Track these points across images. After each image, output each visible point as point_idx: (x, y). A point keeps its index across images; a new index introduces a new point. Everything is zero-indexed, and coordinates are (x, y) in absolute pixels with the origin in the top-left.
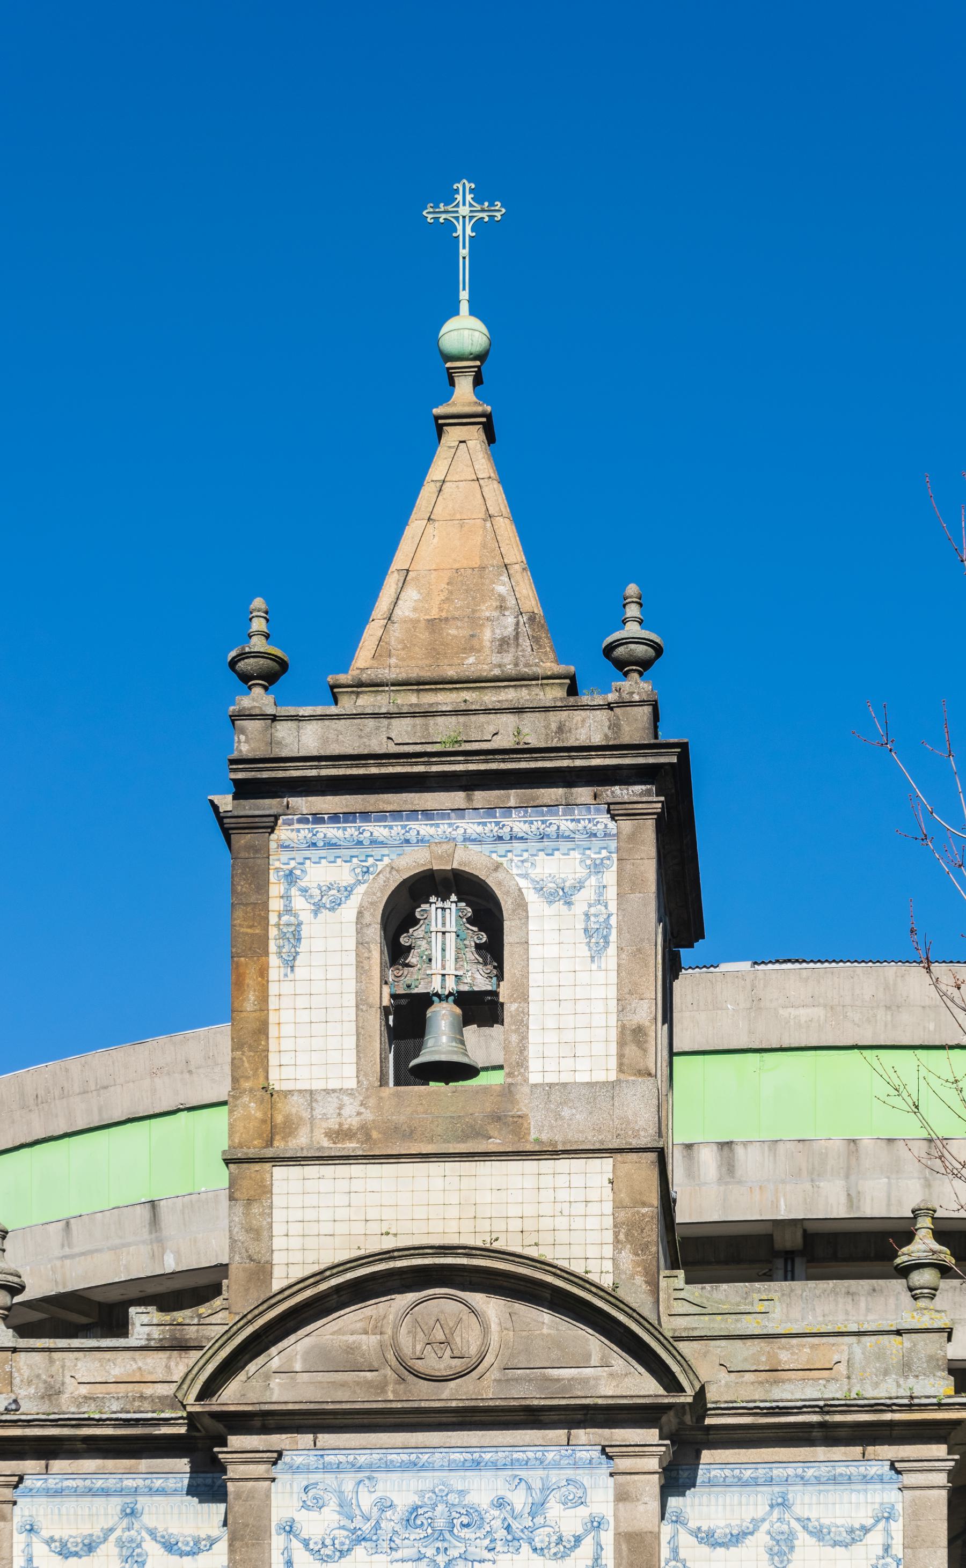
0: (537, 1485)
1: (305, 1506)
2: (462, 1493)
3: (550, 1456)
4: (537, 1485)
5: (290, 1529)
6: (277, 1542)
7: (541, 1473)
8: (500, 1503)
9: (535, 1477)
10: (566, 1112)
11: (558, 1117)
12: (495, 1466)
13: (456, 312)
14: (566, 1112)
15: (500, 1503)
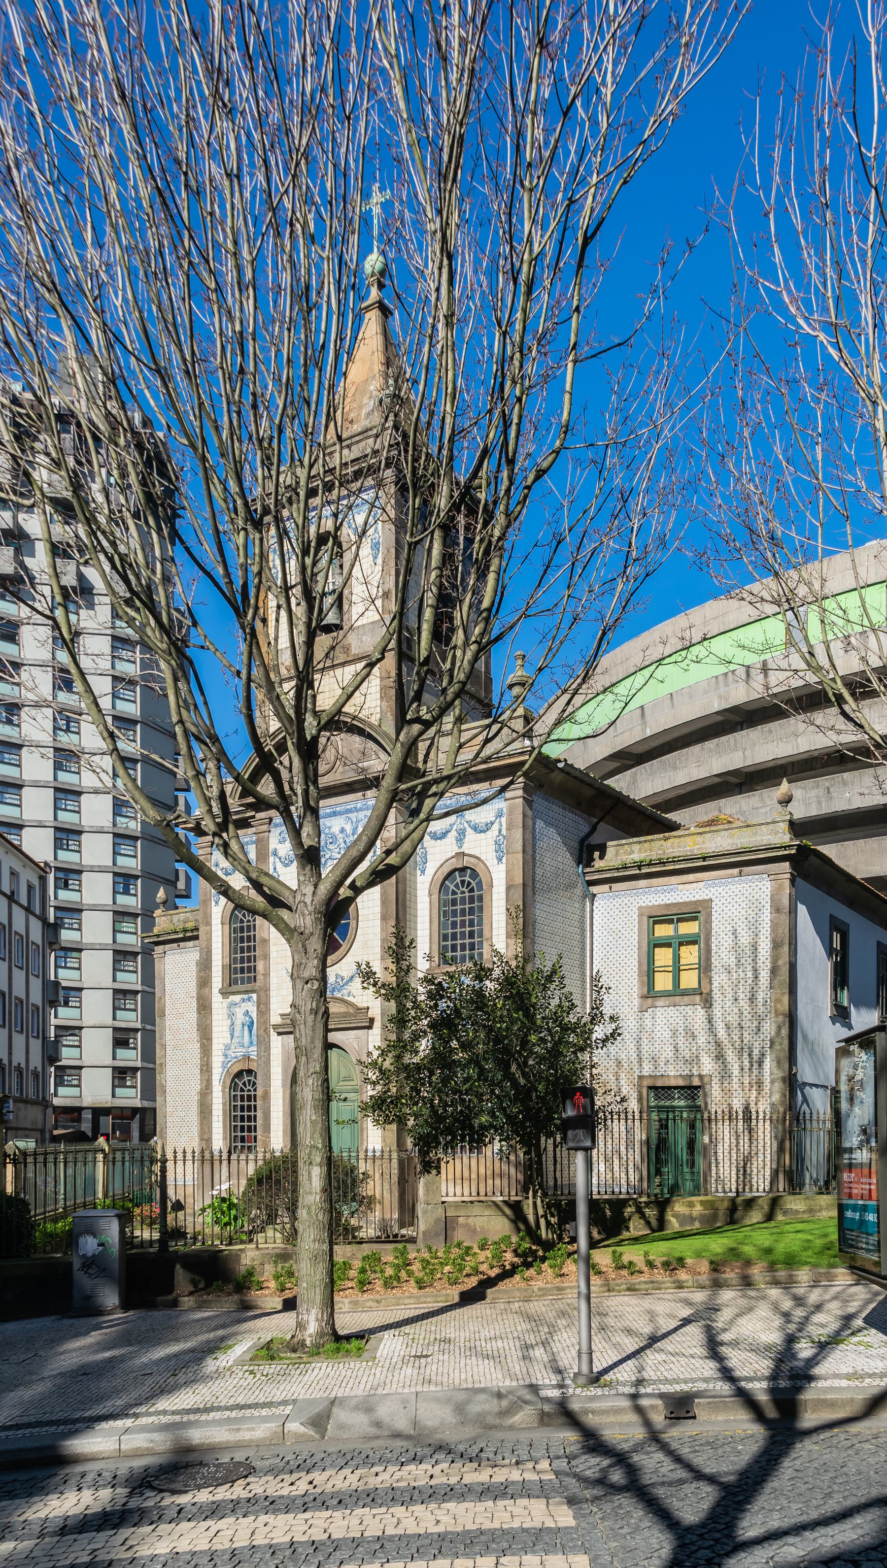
0: (354, 820)
1: (280, 842)
2: (330, 828)
3: (359, 805)
4: (354, 820)
5: (275, 854)
6: (271, 859)
7: (355, 814)
8: (342, 830)
9: (353, 816)
10: (364, 638)
11: (362, 641)
12: (340, 813)
13: (372, 251)
14: (364, 638)
15: (342, 830)
